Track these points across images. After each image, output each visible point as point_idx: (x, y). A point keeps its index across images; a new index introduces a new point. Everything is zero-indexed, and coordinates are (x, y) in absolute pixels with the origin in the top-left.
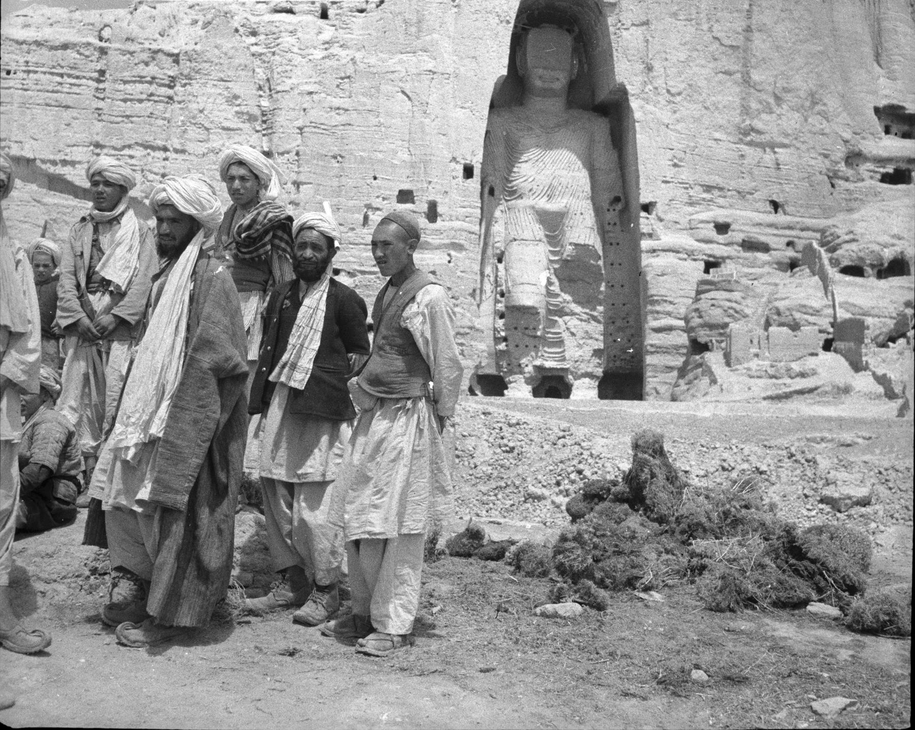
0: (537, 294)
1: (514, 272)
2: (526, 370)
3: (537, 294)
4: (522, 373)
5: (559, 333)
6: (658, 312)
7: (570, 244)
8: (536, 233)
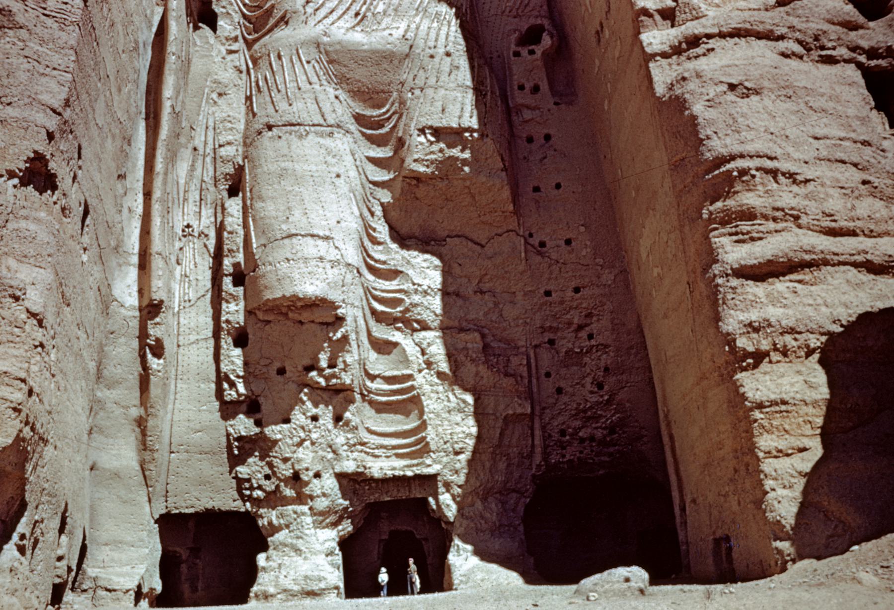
0: (334, 263)
1: (268, 209)
2: (315, 487)
3: (334, 263)
4: (301, 499)
5: (410, 377)
6: (749, 215)
7: (422, 131)
8: (327, 108)
